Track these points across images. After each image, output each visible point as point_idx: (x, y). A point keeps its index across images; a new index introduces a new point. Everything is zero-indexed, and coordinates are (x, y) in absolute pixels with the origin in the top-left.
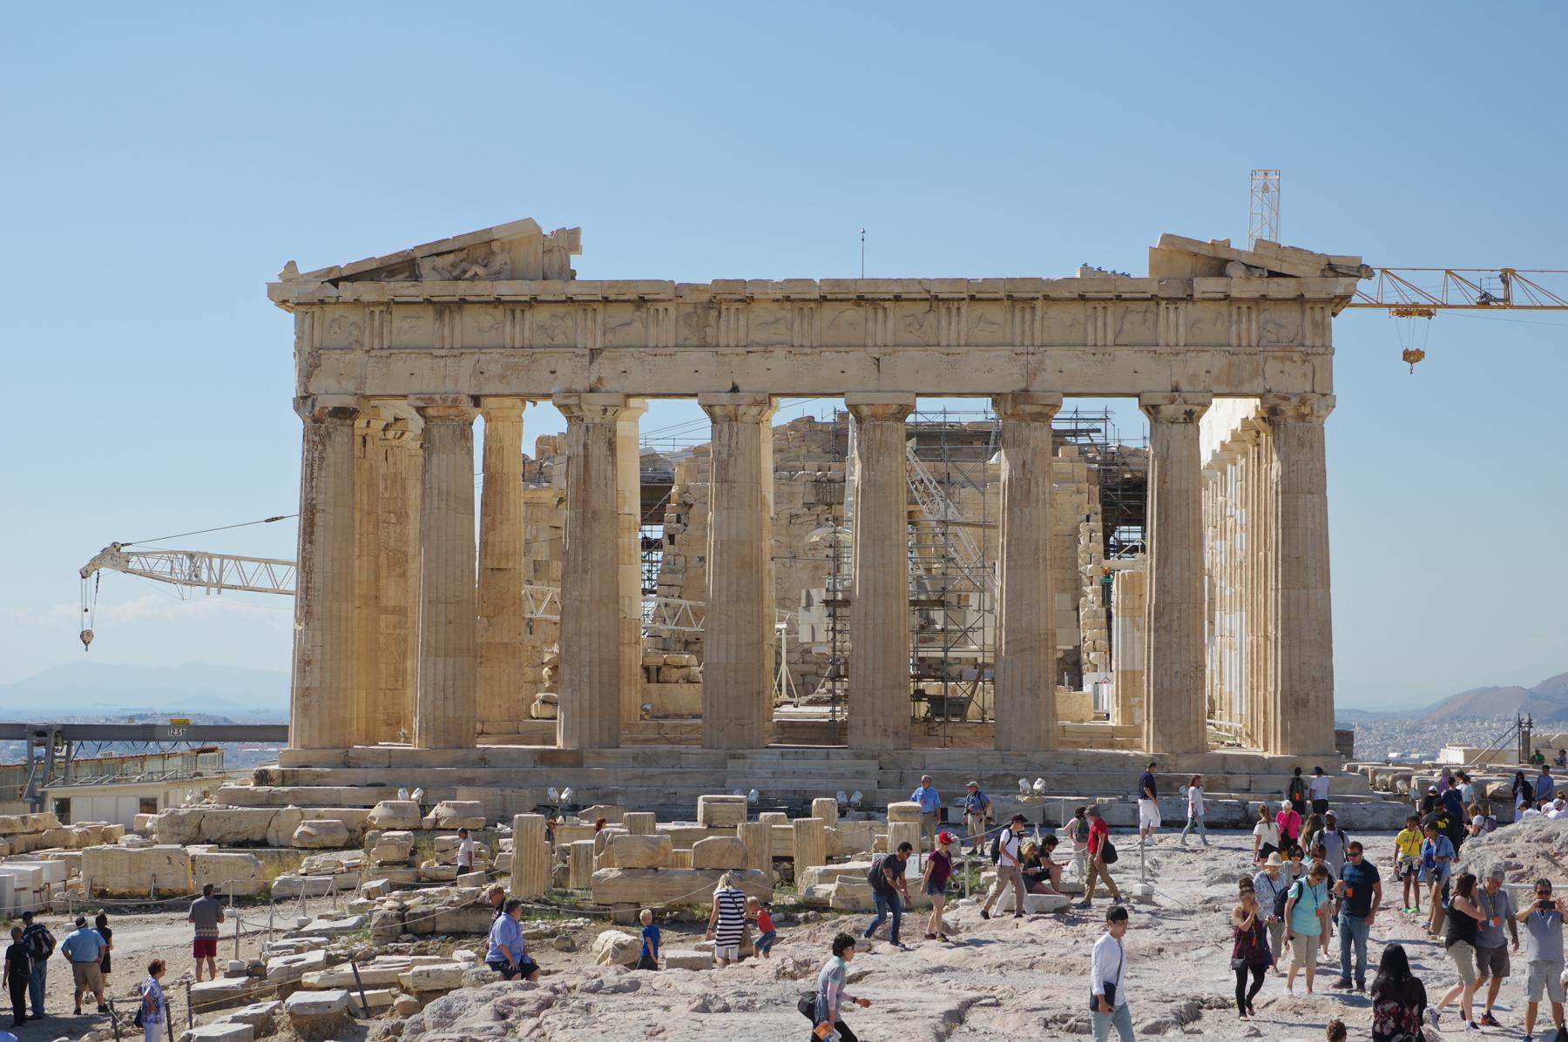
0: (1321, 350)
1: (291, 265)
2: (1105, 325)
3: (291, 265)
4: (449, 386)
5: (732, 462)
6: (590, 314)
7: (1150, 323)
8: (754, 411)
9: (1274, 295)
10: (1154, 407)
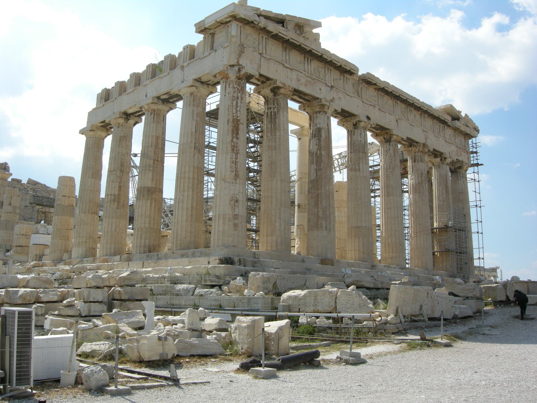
10: (445, 158)
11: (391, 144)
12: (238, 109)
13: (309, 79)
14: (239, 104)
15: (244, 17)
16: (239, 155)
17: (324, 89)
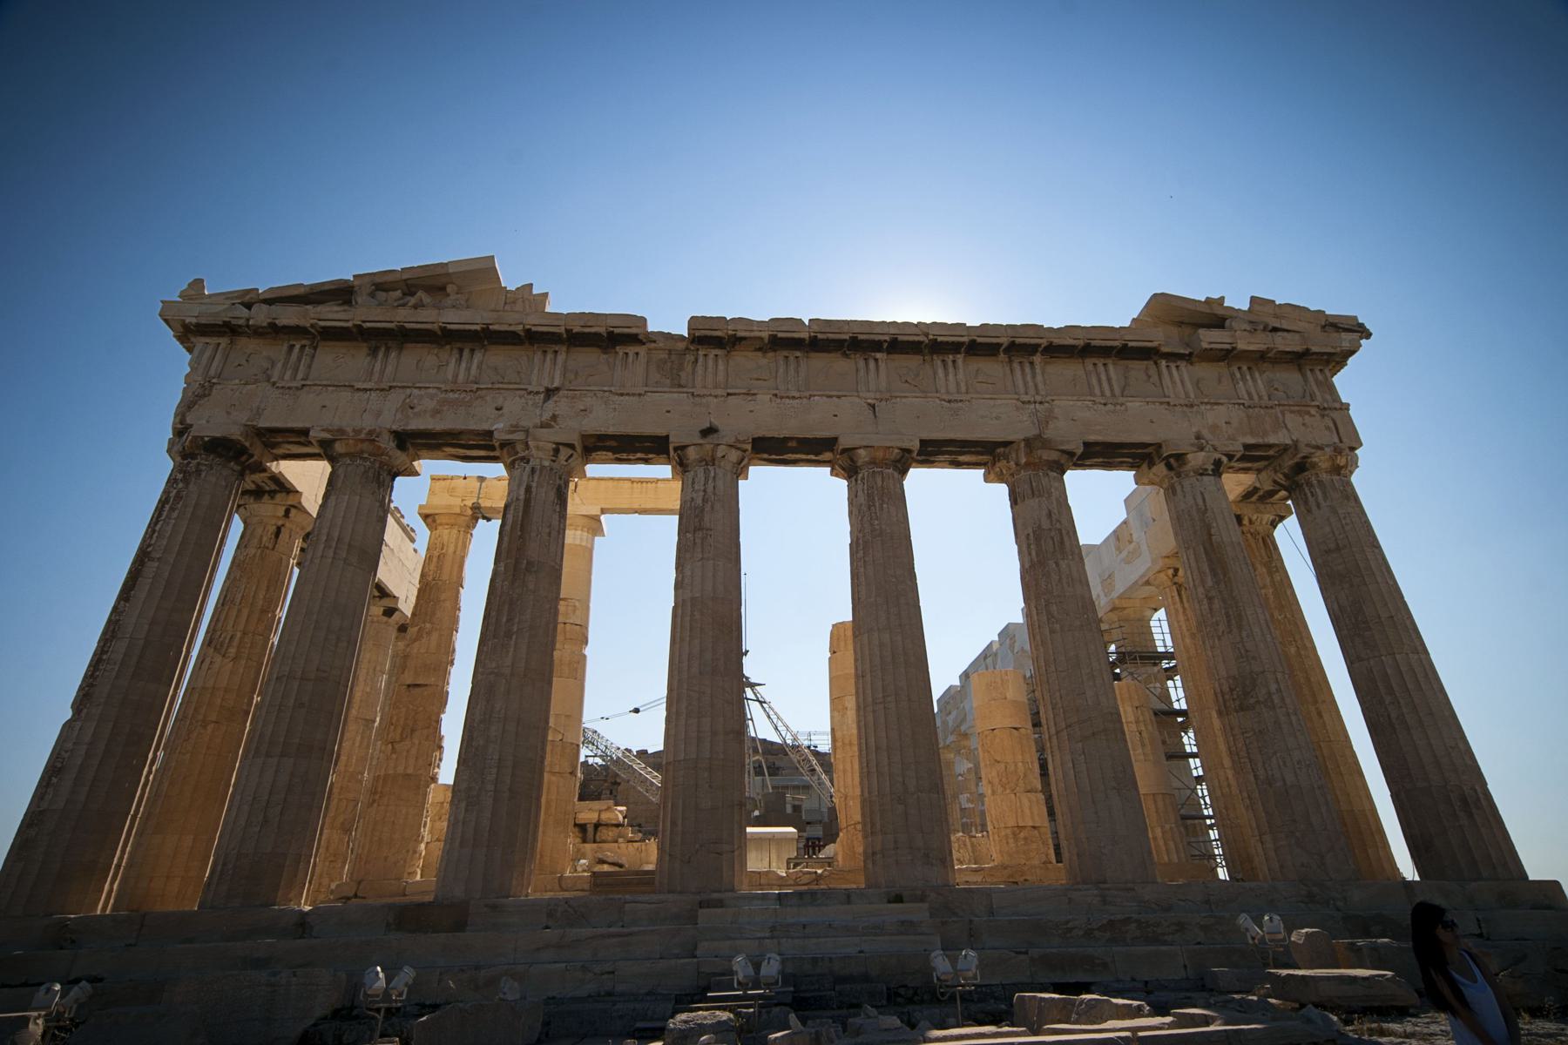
0: (1337, 405)
2: (1109, 380)
4: (368, 423)
5: (708, 508)
7: (1155, 378)
8: (734, 455)
9: (1282, 348)
10: (1180, 457)
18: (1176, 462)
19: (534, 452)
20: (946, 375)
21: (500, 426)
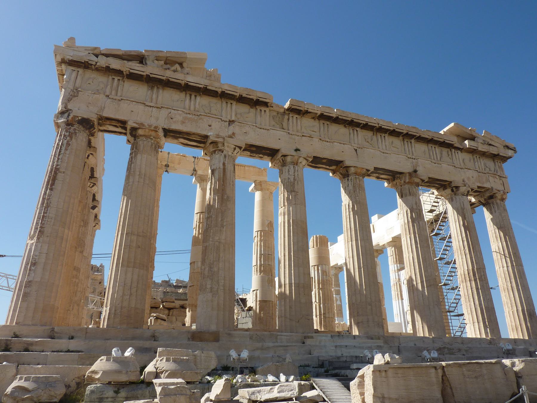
1: (72, 39)
2: (436, 154)
3: (72, 39)
4: (153, 122)
5: (296, 182)
6: (229, 105)
7: (450, 156)
8: (304, 162)
10: (457, 188)
11: (350, 178)
12: (60, 157)
13: (191, 116)
14: (63, 152)
15: (71, 58)
16: (49, 209)
17: (216, 124)
18: (455, 189)
19: (226, 148)
20: (382, 142)
21: (212, 133)
